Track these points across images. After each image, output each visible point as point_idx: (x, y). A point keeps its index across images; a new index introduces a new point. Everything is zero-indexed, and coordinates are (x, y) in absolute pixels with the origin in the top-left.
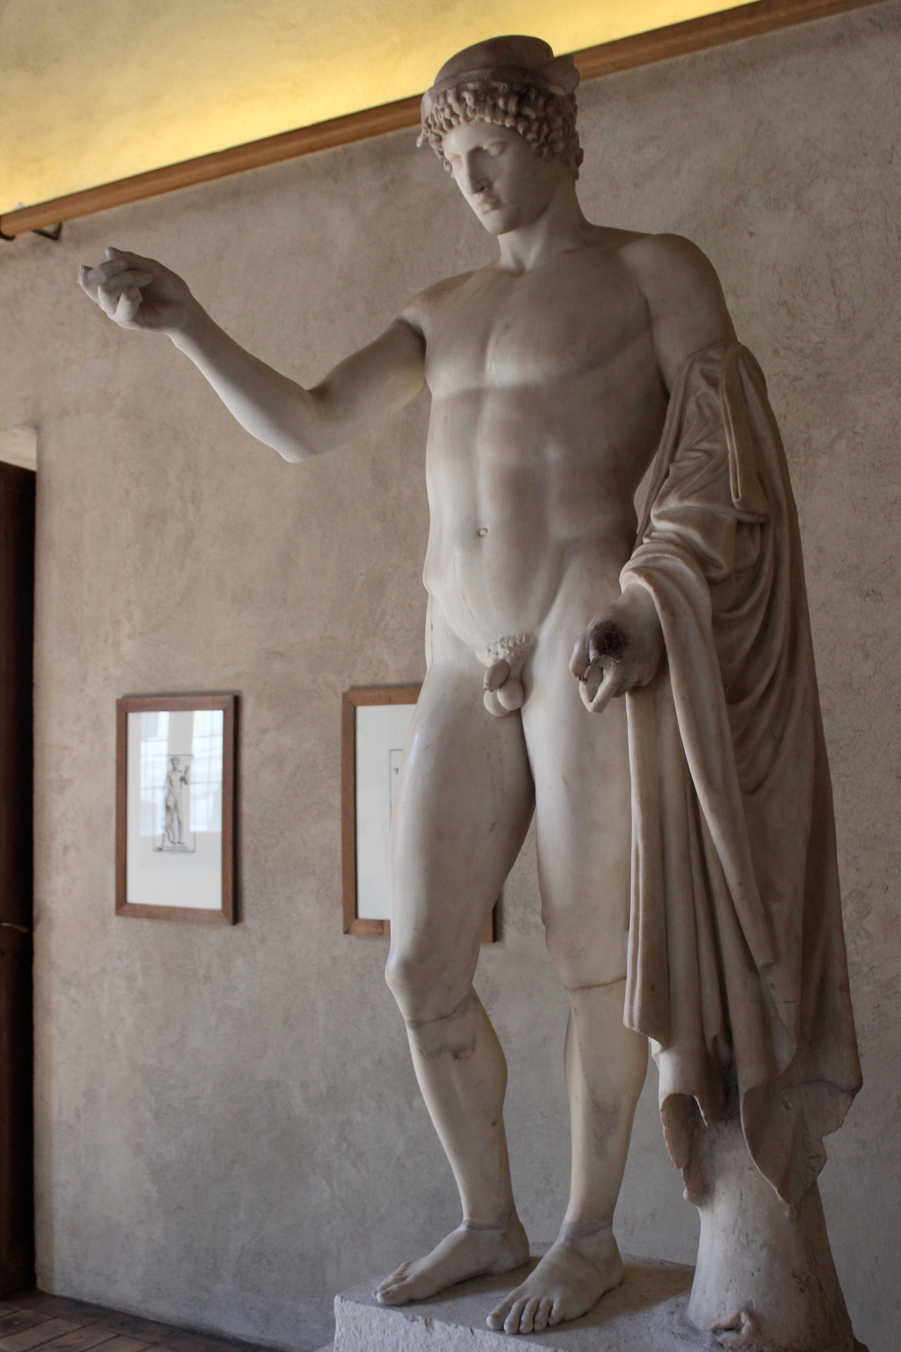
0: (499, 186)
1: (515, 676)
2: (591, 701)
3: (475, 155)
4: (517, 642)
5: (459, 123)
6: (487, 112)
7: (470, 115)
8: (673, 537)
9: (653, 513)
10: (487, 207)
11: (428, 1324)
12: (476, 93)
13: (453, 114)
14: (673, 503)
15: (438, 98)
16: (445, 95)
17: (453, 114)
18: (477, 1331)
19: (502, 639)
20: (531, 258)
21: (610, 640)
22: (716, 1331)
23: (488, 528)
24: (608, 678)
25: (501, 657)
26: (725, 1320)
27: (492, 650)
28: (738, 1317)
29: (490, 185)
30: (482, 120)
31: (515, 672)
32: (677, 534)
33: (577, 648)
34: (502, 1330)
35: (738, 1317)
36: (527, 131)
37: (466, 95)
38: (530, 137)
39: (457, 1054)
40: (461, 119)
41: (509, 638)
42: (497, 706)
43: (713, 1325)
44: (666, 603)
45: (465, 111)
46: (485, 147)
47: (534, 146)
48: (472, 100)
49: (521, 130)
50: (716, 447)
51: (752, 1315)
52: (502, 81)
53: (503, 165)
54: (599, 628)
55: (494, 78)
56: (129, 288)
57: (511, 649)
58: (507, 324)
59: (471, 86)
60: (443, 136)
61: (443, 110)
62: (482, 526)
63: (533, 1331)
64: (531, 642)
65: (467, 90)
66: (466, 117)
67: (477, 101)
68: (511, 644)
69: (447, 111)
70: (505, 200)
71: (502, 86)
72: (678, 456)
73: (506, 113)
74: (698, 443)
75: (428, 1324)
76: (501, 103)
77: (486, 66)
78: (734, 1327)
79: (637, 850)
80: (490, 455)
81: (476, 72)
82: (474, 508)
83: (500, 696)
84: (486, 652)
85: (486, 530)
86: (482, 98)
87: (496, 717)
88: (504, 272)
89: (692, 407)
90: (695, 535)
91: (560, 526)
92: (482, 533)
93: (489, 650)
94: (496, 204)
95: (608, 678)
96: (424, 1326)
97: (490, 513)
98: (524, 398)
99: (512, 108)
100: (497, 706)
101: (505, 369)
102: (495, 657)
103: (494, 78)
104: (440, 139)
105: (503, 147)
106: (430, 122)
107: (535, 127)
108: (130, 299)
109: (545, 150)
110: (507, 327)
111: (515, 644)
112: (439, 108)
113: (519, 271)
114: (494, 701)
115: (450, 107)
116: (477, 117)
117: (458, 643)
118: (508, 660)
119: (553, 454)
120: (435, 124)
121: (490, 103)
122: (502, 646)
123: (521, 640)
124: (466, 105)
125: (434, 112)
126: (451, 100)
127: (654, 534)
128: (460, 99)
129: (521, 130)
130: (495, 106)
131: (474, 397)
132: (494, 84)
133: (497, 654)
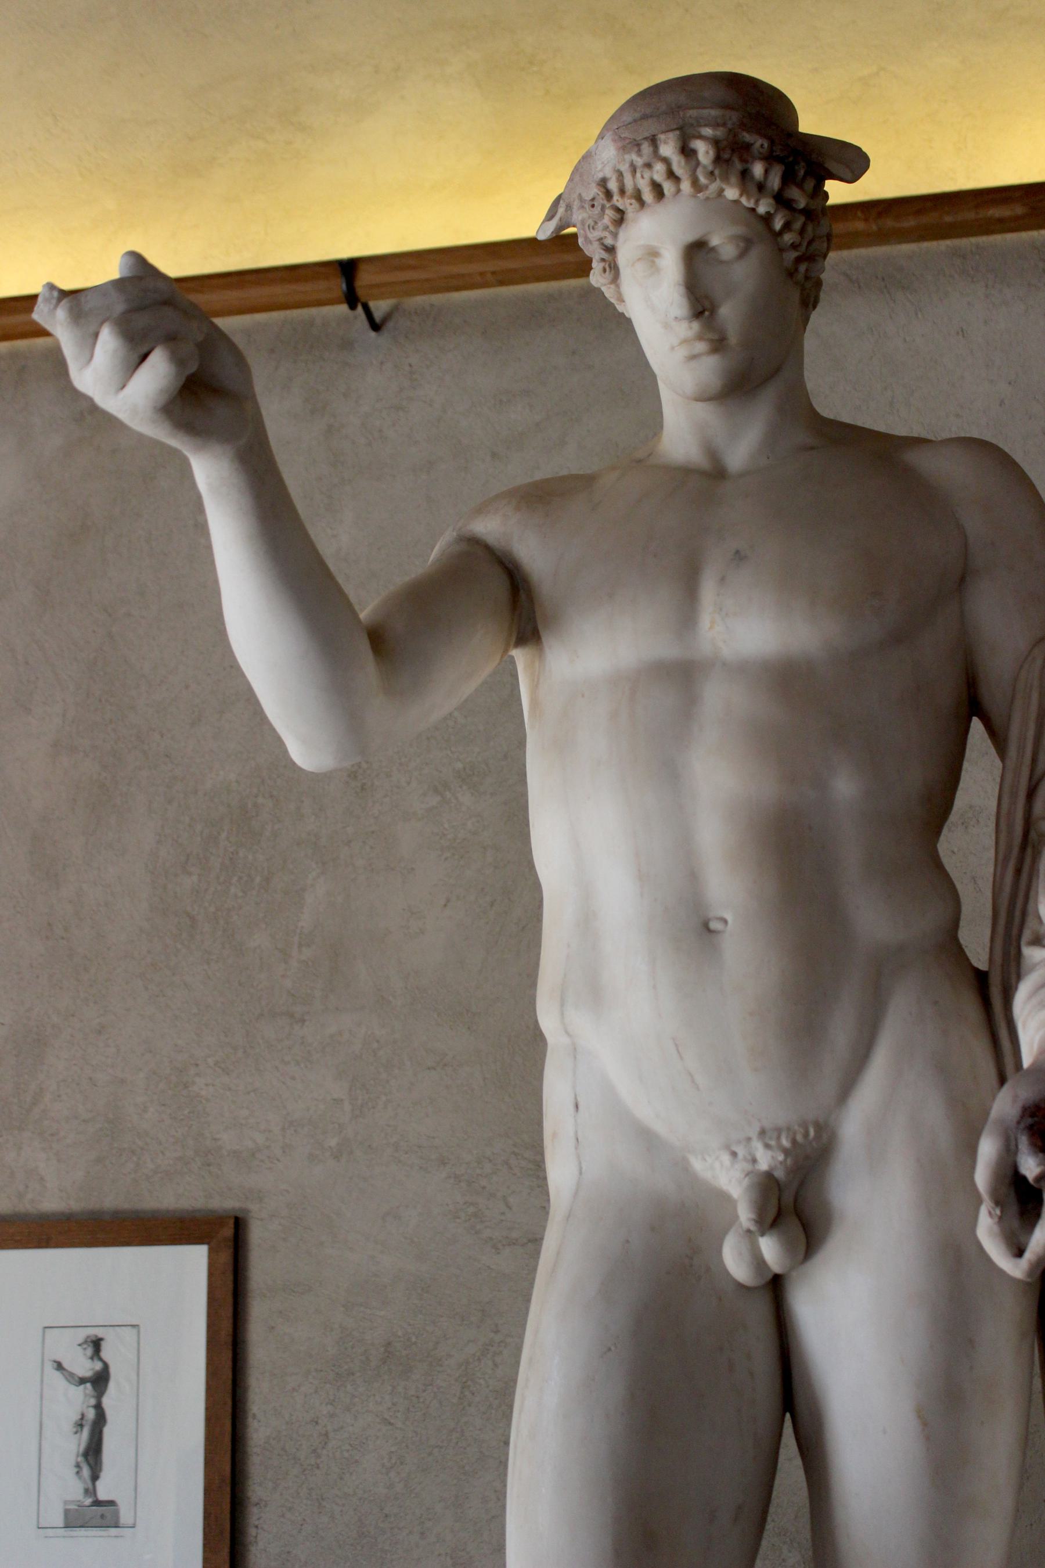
0: (729, 312)
1: (796, 1206)
2: (1019, 1253)
3: (696, 252)
4: (799, 1138)
5: (679, 191)
6: (733, 179)
7: (703, 180)
10: (701, 347)
12: (716, 143)
13: (671, 175)
15: (638, 145)
16: (653, 141)
17: (671, 175)
19: (763, 1133)
20: (739, 454)
23: (729, 917)
25: (763, 1165)
27: (741, 1151)
29: (713, 310)
30: (720, 192)
31: (788, 1198)
33: (988, 1149)
36: (787, 226)
38: (788, 238)
40: (686, 186)
41: (779, 1131)
45: (694, 171)
46: (715, 241)
47: (793, 255)
48: (712, 153)
49: (778, 224)
52: (760, 133)
53: (742, 276)
55: (743, 126)
56: (171, 339)
57: (786, 1152)
58: (737, 552)
59: (708, 131)
60: (630, 214)
61: (648, 166)
62: (711, 914)
64: (825, 1137)
65: (701, 137)
66: (695, 182)
67: (718, 160)
68: (785, 1143)
69: (659, 168)
70: (733, 339)
71: (759, 143)
73: (761, 187)
76: (758, 170)
80: (720, 783)
81: (714, 112)
82: (693, 877)
84: (726, 1158)
85: (725, 921)
86: (726, 156)
87: (740, 1286)
88: (685, 472)
91: (875, 919)
92: (714, 925)
93: (734, 1154)
94: (719, 345)
97: (730, 890)
98: (786, 680)
99: (775, 182)
100: (759, 1262)
101: (747, 626)
102: (748, 1167)
103: (743, 126)
105: (746, 245)
106: (613, 185)
107: (797, 225)
108: (178, 360)
109: (802, 268)
111: (794, 1142)
112: (639, 161)
113: (716, 473)
114: (741, 1255)
115: (666, 161)
116: (714, 187)
117: (647, 1139)
118: (779, 1174)
119: (845, 787)
120: (622, 192)
121: (738, 166)
122: (767, 1146)
123: (806, 1135)
124: (698, 163)
125: (625, 168)
126: (668, 149)
128: (687, 152)
129: (778, 224)
130: (745, 175)
131: (681, 677)
132: (747, 137)
133: (754, 1161)
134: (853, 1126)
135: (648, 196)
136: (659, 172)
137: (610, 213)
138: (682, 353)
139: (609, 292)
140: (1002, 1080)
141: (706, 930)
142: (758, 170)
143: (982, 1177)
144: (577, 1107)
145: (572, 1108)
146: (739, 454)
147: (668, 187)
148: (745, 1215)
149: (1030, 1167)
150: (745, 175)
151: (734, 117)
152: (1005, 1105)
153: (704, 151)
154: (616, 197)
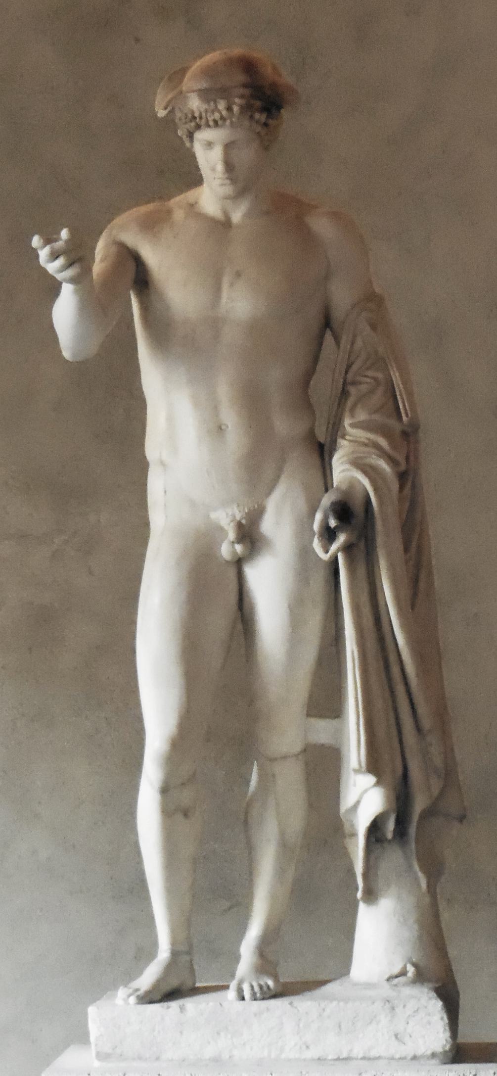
2: (327, 552)
3: (228, 147)
8: (366, 441)
9: (347, 422)
10: (228, 182)
11: (182, 1009)
12: (241, 106)
13: (222, 118)
14: (362, 416)
17: (222, 118)
18: (224, 1004)
21: (343, 511)
22: (388, 980)
24: (342, 538)
25: (238, 518)
26: (397, 970)
28: (405, 967)
32: (369, 439)
33: (319, 516)
34: (243, 999)
35: (405, 967)
37: (236, 109)
39: (186, 814)
42: (234, 552)
43: (387, 977)
44: (376, 490)
50: (380, 375)
51: (415, 965)
54: (334, 504)
59: (237, 100)
63: (263, 999)
67: (242, 113)
71: (258, 103)
72: (350, 377)
73: (257, 122)
74: (368, 369)
75: (182, 1009)
77: (245, 86)
78: (403, 973)
79: (353, 653)
83: (239, 548)
88: (212, 221)
89: (359, 343)
90: (383, 442)
92: (223, 427)
95: (342, 538)
96: (179, 1010)
98: (255, 329)
100: (234, 552)
104: (198, 127)
110: (238, 274)
113: (226, 224)
114: (227, 549)
115: (219, 112)
118: (244, 521)
121: (249, 114)
127: (347, 437)
128: (229, 109)
130: (252, 117)
132: (252, 102)
134: (272, 504)
135: (211, 123)
136: (217, 116)
137: (193, 124)
138: (218, 182)
139: (188, 144)
140: (327, 490)
141: (220, 429)
142: (257, 116)
143: (316, 526)
144: (165, 492)
145: (163, 493)
146: (237, 216)
147: (220, 122)
148: (232, 535)
149: (333, 523)
150: (252, 117)
151: (247, 92)
152: (327, 500)
153: (236, 109)
154: (198, 120)
